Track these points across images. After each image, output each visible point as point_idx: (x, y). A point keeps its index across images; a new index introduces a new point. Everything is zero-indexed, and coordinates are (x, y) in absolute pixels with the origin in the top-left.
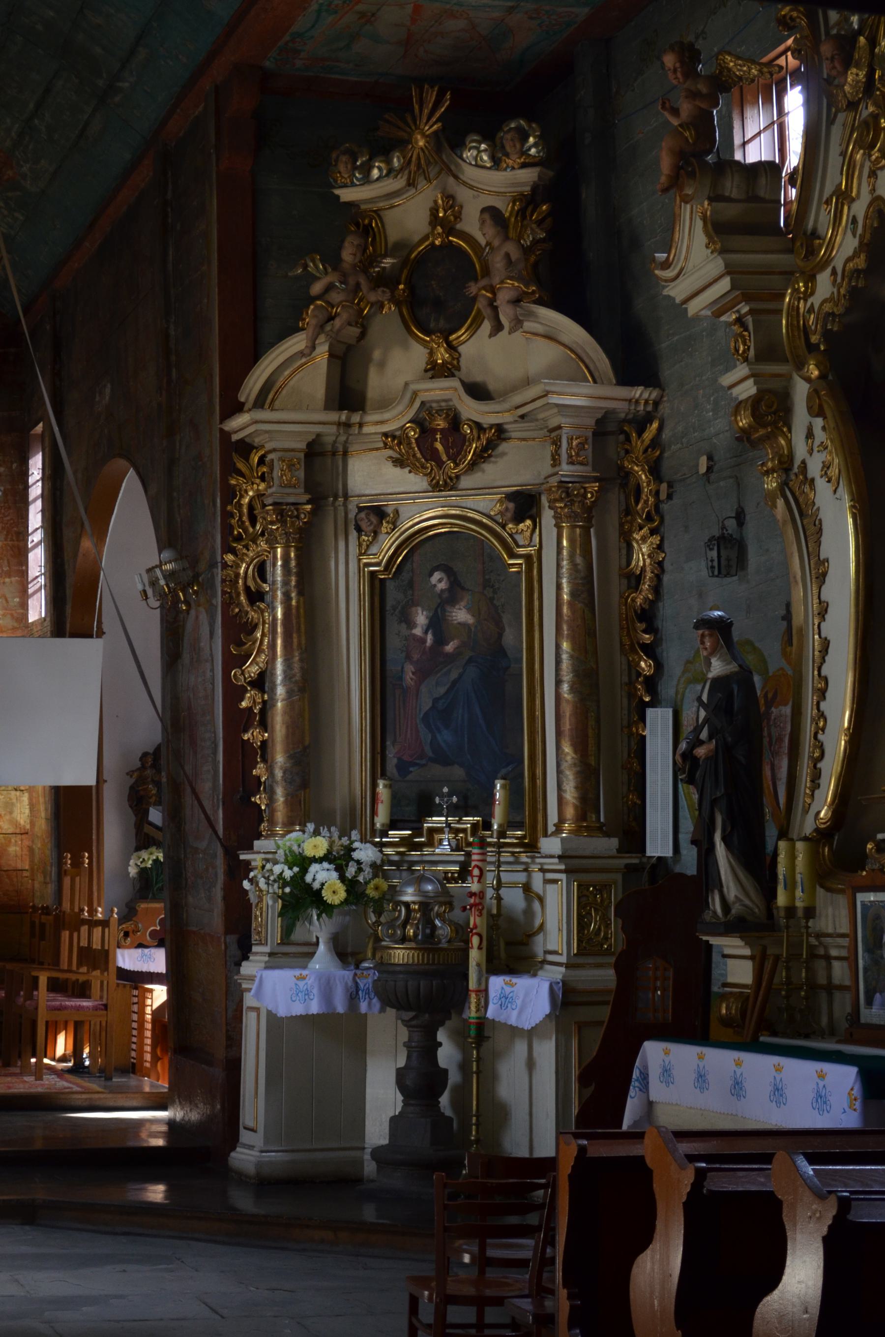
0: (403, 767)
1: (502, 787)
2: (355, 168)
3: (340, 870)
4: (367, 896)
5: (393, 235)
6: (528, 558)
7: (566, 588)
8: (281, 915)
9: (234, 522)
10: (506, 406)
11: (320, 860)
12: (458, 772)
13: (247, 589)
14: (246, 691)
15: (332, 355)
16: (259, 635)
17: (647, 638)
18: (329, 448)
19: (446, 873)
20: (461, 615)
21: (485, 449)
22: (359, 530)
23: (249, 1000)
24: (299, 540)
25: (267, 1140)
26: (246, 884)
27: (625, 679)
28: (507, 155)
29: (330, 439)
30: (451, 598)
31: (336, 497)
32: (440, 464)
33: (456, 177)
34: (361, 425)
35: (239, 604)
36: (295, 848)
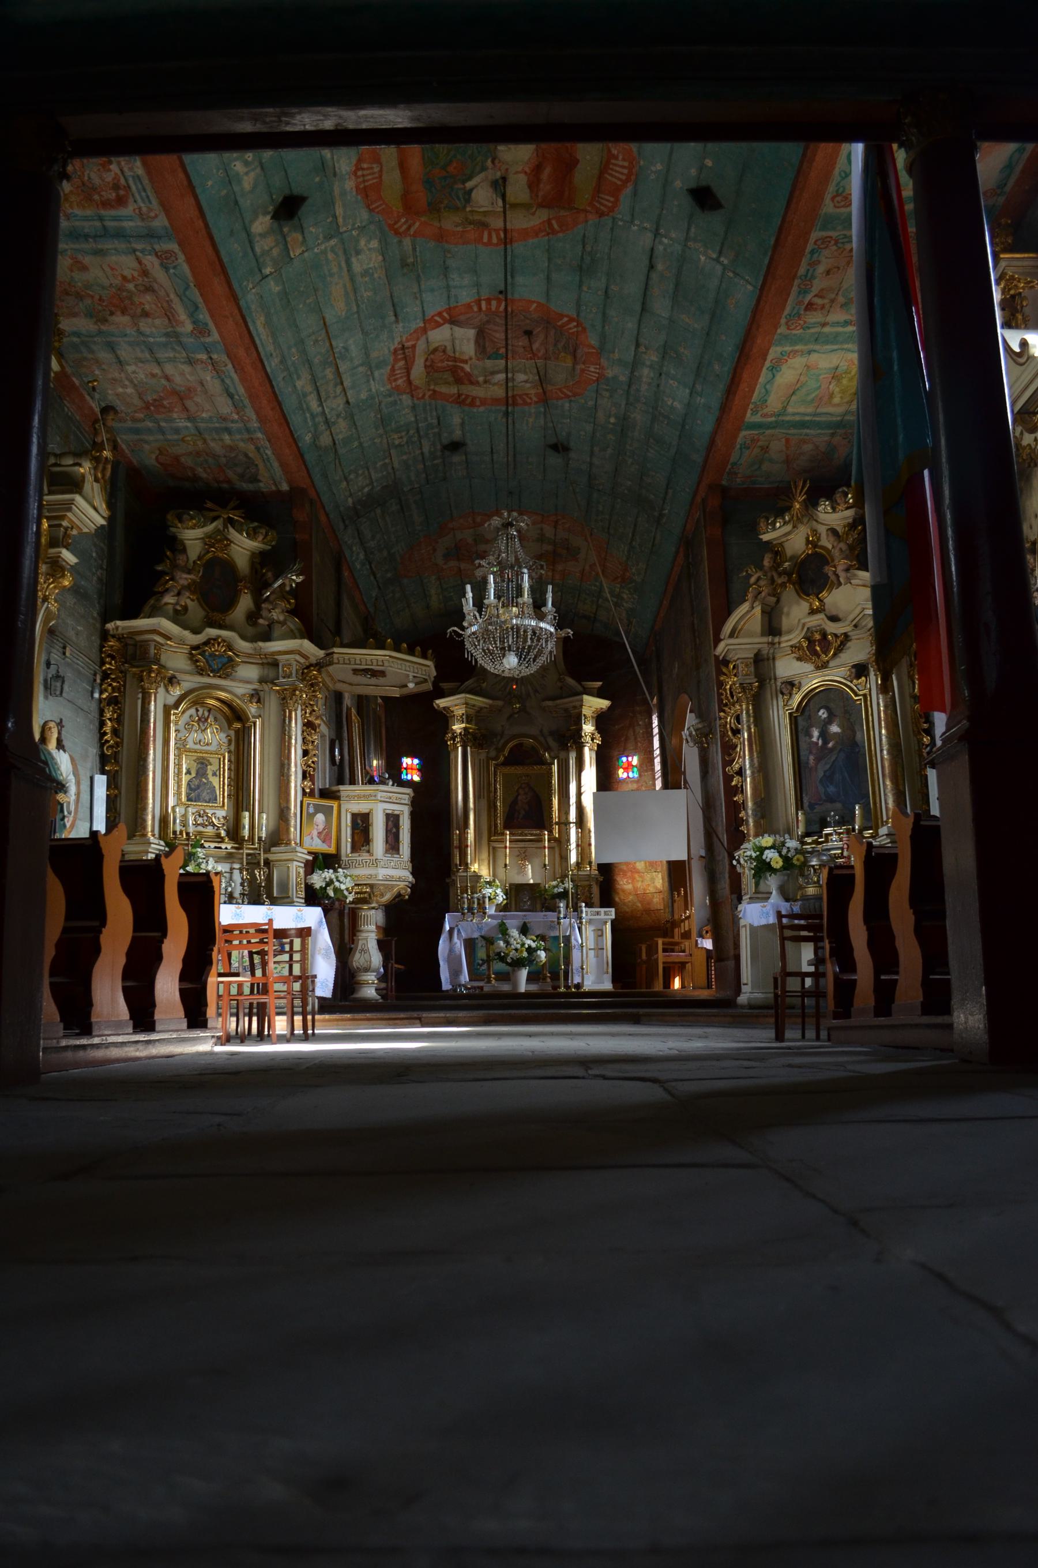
0: (812, 806)
1: (859, 807)
2: (768, 524)
3: (780, 853)
4: (793, 864)
5: (789, 553)
6: (865, 696)
7: (882, 704)
8: (754, 878)
9: (723, 697)
10: (847, 623)
11: (769, 848)
12: (838, 805)
13: (731, 728)
14: (734, 777)
15: (763, 612)
16: (738, 750)
17: (926, 726)
18: (766, 656)
19: (835, 854)
20: (835, 729)
21: (840, 646)
22: (783, 694)
23: (742, 922)
24: (754, 700)
25: (752, 988)
26: (735, 863)
27: (917, 748)
28: (838, 504)
29: (765, 652)
30: (829, 721)
31: (770, 680)
32: (819, 656)
33: (817, 521)
34: (779, 643)
35: (728, 736)
36: (757, 843)
